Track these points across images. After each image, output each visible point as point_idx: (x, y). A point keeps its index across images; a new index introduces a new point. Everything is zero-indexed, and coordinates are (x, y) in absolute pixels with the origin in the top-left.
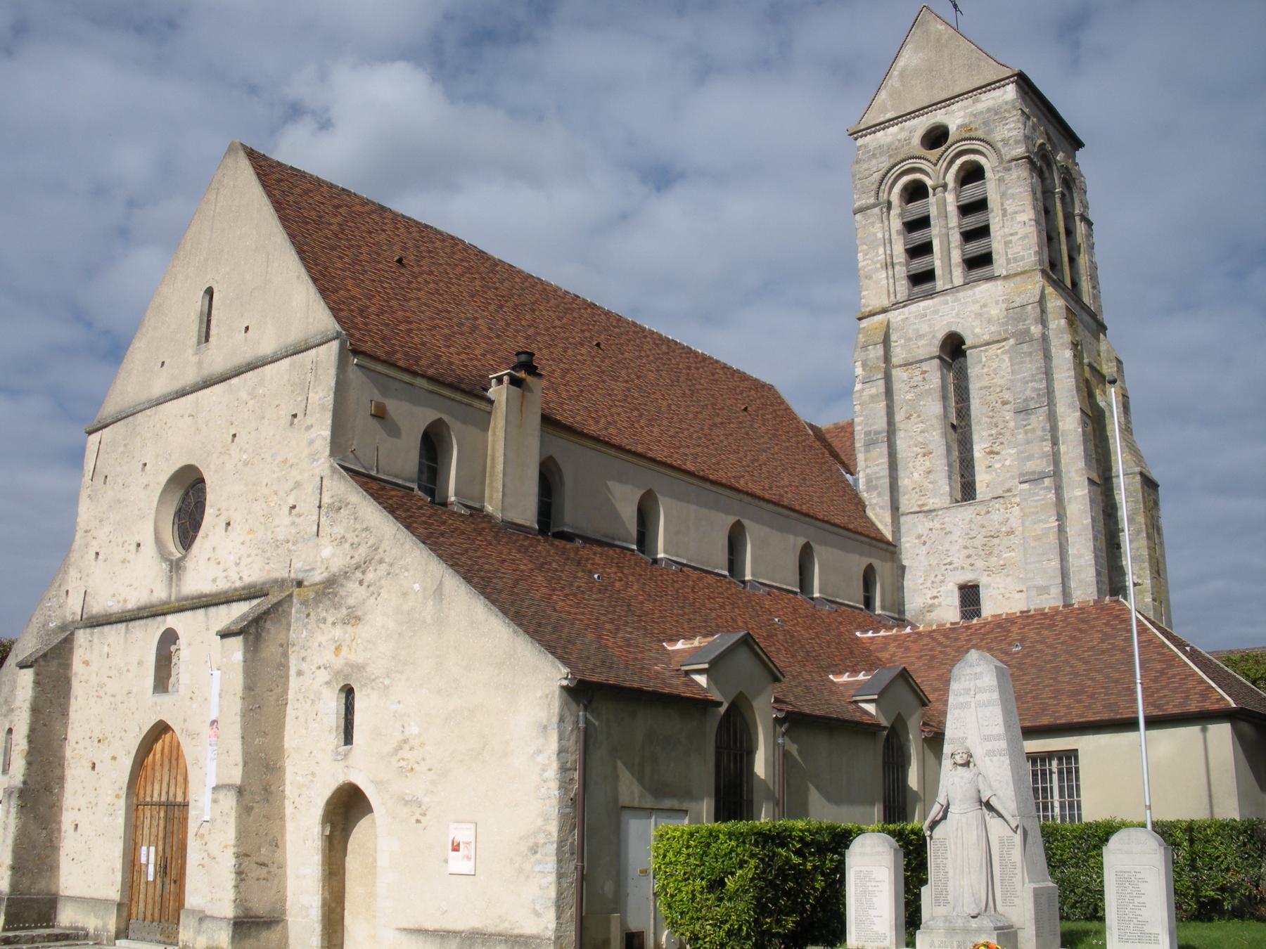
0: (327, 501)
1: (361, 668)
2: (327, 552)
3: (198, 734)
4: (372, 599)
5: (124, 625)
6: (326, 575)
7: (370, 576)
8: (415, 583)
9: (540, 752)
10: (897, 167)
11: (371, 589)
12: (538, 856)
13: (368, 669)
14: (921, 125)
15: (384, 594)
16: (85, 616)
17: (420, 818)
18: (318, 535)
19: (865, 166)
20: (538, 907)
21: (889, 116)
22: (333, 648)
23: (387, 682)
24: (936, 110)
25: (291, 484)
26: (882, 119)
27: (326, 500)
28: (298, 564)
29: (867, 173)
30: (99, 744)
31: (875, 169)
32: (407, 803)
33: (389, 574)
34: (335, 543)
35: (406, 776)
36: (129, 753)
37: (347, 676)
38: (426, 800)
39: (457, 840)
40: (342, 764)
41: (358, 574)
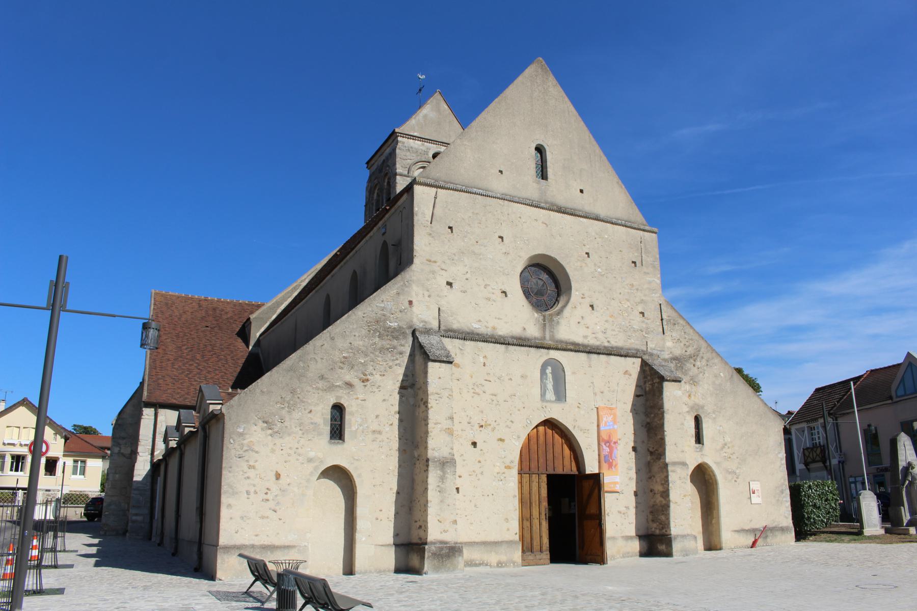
0: (666, 317)
1: (702, 407)
2: (669, 344)
3: (588, 430)
4: (701, 375)
5: (503, 346)
6: (671, 355)
7: (698, 364)
8: (721, 372)
9: (779, 453)
10: (421, 163)
11: (700, 370)
12: (784, 495)
13: (705, 408)
14: (434, 148)
15: (707, 375)
16: (442, 328)
17: (736, 479)
18: (664, 334)
19: (404, 153)
20: (786, 515)
21: (415, 134)
22: (687, 395)
23: (714, 416)
24: (441, 145)
25: (638, 300)
26: (412, 134)
27: (665, 317)
28: (651, 345)
29: (405, 158)
30: (481, 429)
31: (409, 158)
32: (730, 473)
33: (707, 365)
34: (675, 341)
35: (728, 460)
36: (519, 437)
37: (697, 410)
38: (737, 471)
39: (754, 489)
40: (700, 453)
41: (692, 361)
